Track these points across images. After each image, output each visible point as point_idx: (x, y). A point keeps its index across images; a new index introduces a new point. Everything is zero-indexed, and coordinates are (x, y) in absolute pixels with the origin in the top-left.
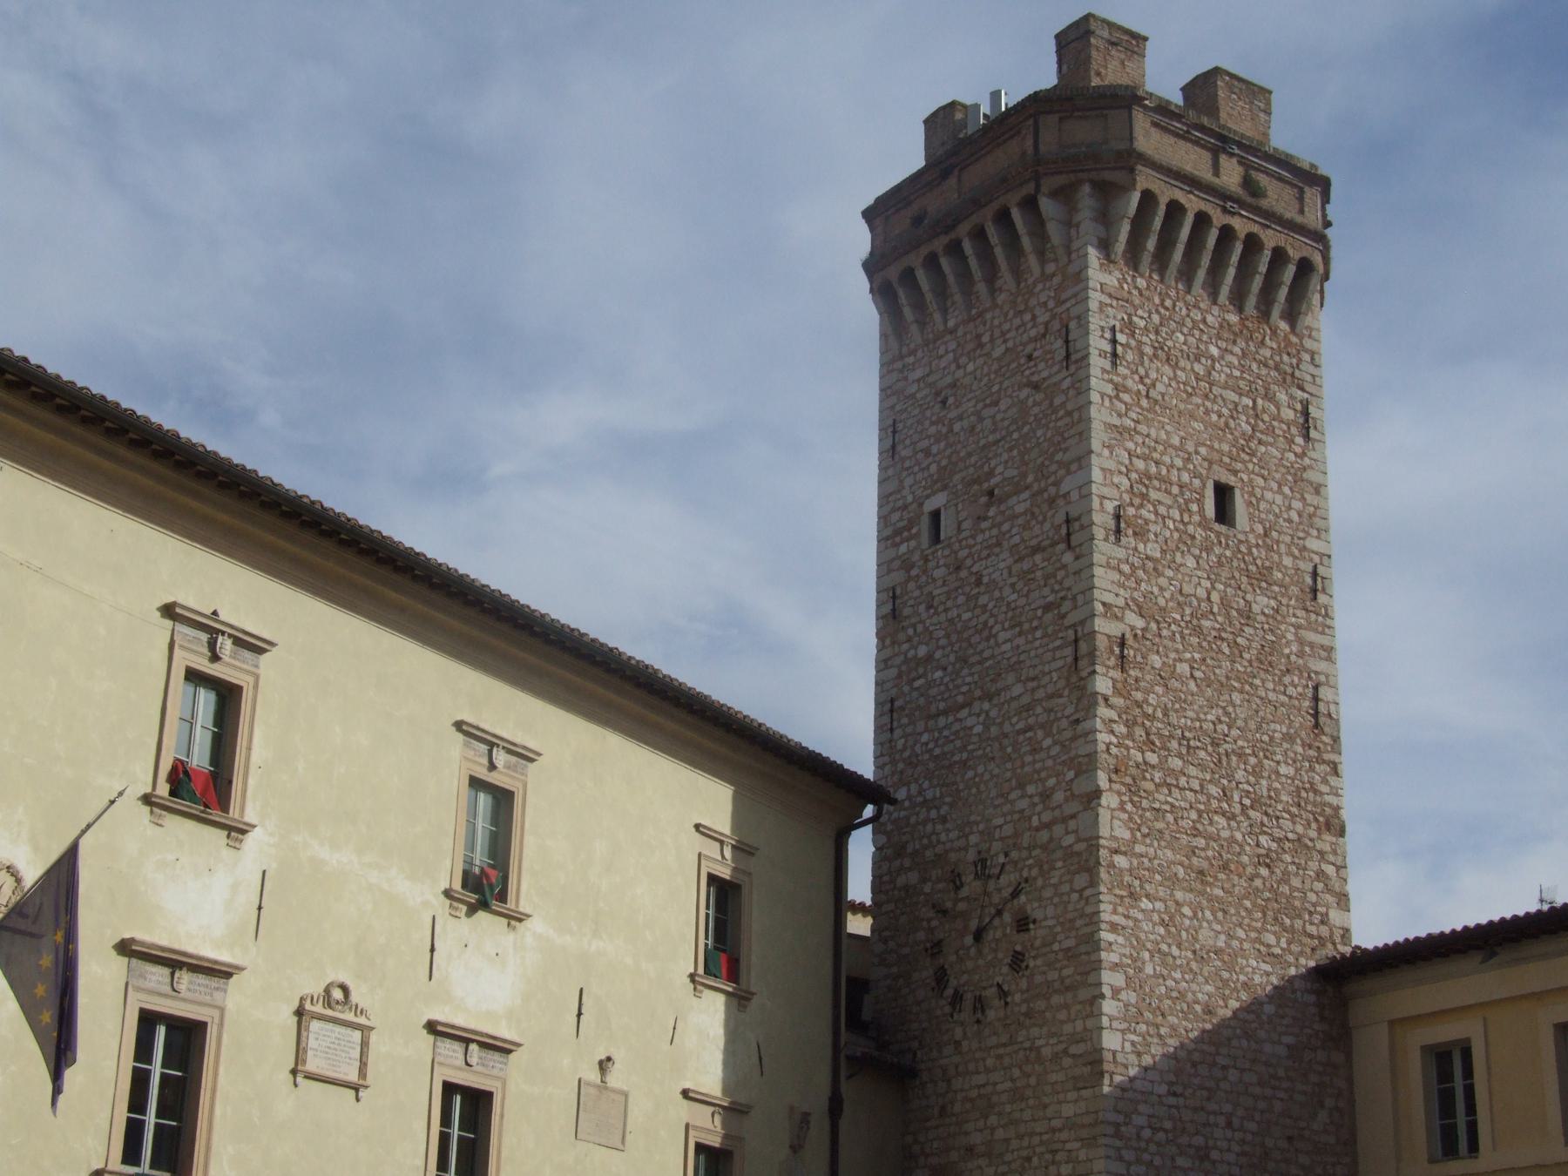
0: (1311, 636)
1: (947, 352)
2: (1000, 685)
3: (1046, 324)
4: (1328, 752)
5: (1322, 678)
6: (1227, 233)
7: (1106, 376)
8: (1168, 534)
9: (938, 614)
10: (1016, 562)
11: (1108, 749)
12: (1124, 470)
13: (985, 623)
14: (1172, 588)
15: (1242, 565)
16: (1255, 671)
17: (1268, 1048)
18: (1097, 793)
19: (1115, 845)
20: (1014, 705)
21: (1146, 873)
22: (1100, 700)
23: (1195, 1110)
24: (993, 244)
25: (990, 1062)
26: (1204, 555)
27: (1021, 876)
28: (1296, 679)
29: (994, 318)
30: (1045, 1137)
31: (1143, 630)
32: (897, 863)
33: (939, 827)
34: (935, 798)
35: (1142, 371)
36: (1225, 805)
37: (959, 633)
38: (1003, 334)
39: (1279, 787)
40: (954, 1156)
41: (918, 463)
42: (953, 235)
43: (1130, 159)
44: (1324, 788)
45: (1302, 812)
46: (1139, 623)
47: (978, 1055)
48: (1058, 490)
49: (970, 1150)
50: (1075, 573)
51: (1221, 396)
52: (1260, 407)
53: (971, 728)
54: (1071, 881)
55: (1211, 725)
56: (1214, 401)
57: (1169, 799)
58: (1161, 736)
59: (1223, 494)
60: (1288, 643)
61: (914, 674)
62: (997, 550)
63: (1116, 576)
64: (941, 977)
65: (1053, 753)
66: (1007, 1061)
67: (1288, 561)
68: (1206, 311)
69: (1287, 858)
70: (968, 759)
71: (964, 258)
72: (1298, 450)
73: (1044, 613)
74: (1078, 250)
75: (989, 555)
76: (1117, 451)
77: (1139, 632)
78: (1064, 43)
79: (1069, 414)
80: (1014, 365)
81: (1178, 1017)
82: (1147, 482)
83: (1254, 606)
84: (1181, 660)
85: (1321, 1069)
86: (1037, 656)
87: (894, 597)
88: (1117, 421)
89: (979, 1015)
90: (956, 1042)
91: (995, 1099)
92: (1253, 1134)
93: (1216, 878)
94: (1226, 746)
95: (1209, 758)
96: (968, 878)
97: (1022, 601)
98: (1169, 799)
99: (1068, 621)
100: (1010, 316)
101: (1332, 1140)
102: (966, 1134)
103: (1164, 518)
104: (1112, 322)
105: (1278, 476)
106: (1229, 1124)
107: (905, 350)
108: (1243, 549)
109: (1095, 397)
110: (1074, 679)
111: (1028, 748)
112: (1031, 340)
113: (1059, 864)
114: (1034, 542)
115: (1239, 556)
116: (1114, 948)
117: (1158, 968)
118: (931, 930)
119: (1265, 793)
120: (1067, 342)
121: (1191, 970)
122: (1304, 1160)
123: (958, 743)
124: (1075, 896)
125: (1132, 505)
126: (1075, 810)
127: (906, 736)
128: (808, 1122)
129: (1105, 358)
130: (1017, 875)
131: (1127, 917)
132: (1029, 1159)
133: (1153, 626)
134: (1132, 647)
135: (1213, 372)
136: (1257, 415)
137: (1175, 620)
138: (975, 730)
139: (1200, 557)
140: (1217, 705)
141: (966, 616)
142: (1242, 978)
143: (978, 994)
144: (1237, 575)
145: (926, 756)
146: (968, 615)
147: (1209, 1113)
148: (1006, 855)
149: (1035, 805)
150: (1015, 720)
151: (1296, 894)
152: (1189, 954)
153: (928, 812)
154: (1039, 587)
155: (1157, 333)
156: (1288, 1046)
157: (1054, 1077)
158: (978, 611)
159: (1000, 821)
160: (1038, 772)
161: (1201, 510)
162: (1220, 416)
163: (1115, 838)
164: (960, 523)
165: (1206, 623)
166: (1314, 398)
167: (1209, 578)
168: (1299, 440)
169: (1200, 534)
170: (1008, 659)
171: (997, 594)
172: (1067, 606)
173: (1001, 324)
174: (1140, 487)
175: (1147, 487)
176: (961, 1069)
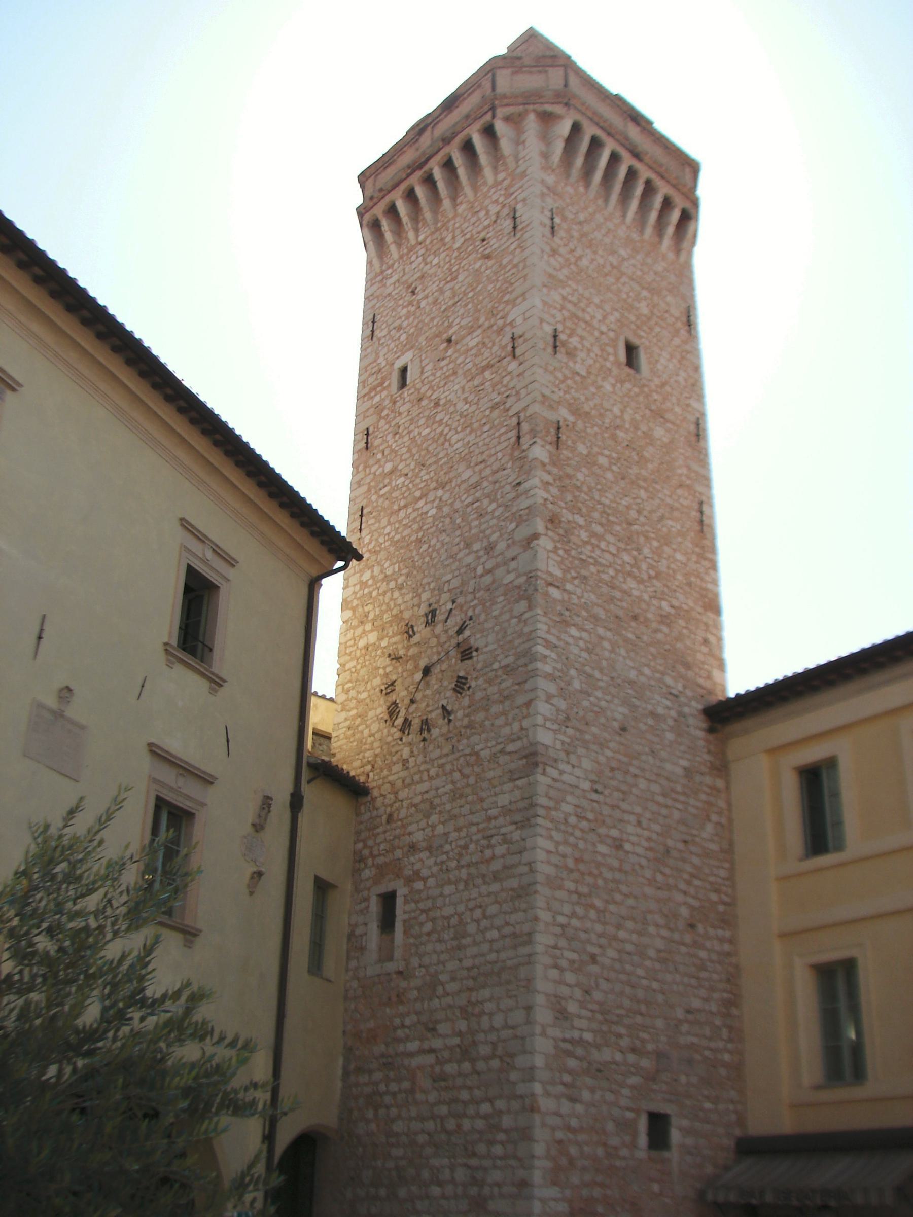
0: (695, 467)
2: (452, 474)
17: (668, 766)
19: (550, 579)
23: (614, 807)
32: (359, 631)
40: (398, 853)
42: (426, 168)
44: (707, 578)
46: (571, 419)
47: (422, 768)
49: (413, 848)
50: (518, 376)
53: (426, 513)
54: (511, 610)
59: (631, 350)
65: (496, 514)
75: (446, 384)
79: (516, 266)
86: (484, 445)
89: (425, 734)
91: (437, 801)
97: (474, 407)
102: (410, 834)
107: (384, 267)
111: (475, 516)
112: (485, 228)
114: (484, 363)
122: (696, 860)
124: (515, 621)
126: (515, 554)
128: (269, 806)
130: (463, 615)
131: (559, 639)
132: (466, 847)
142: (650, 707)
143: (425, 717)
146: (428, 430)
148: (454, 602)
149: (479, 558)
156: (685, 769)
159: (449, 577)
160: (484, 532)
161: (616, 354)
163: (551, 574)
164: (423, 368)
169: (615, 371)
171: (452, 409)
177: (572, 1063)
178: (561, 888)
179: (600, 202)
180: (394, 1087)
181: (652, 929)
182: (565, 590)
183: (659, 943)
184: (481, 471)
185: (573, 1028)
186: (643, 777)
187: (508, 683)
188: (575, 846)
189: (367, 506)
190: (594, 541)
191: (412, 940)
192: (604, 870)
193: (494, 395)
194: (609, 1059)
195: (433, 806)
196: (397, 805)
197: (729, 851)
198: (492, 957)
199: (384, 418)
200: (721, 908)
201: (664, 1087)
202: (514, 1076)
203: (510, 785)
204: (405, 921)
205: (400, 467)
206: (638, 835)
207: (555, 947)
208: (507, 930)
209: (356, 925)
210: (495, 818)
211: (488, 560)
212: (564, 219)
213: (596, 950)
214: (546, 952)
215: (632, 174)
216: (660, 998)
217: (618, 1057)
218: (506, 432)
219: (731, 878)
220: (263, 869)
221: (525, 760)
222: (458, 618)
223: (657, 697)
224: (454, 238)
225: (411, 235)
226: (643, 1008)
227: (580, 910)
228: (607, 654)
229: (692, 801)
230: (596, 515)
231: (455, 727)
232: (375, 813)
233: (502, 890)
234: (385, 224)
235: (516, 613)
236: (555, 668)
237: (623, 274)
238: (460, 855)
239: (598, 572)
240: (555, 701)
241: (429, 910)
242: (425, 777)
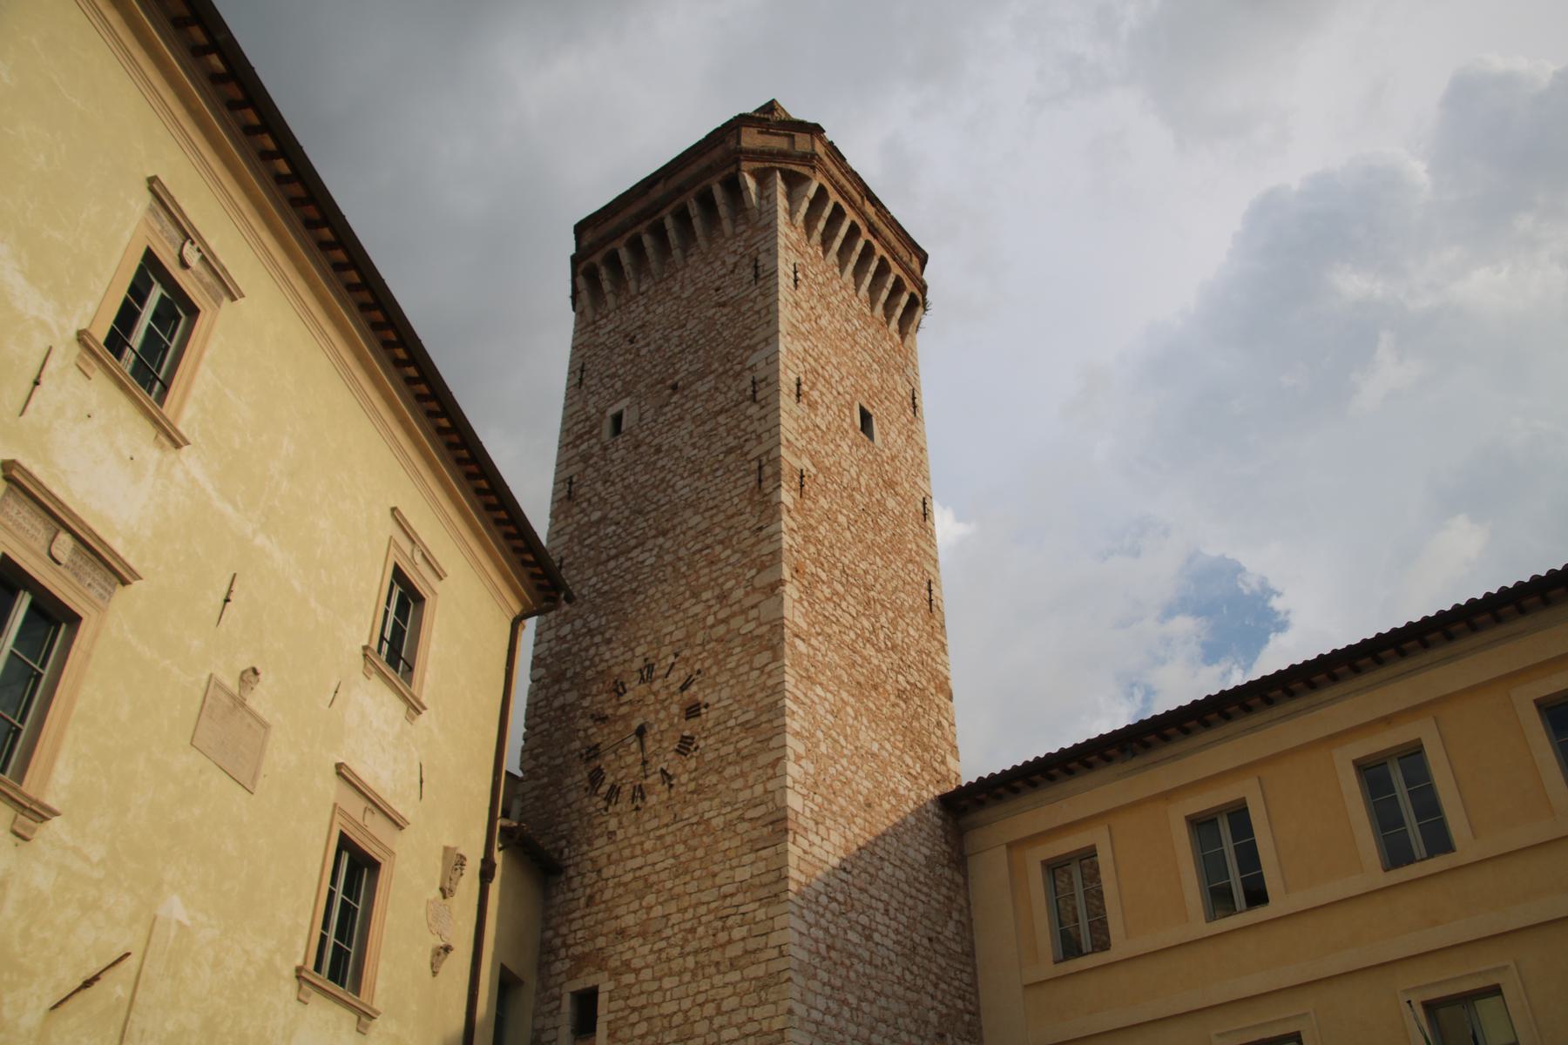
2: (676, 521)
18: (781, 582)
23: (862, 890)
24: (692, 215)
25: (648, 845)
27: (692, 669)
33: (603, 649)
34: (600, 626)
40: (601, 942)
44: (939, 660)
46: (813, 470)
47: (634, 841)
49: (622, 933)
50: (759, 419)
54: (751, 662)
59: (866, 417)
61: (585, 536)
64: (596, 777)
66: (669, 840)
70: (638, 587)
75: (670, 430)
79: (758, 312)
87: (571, 483)
89: (639, 802)
90: (610, 833)
102: (617, 917)
106: (887, 912)
112: (720, 277)
123: (629, 577)
124: (756, 673)
130: (688, 670)
131: (805, 695)
132: (693, 930)
138: (647, 563)
142: (892, 785)
143: (638, 783)
147: (871, 897)
148: (676, 655)
158: (656, 472)
159: (672, 628)
163: (796, 625)
164: (642, 414)
169: (851, 433)
171: (677, 454)
178: (814, 977)
179: (837, 270)
182: (810, 645)
184: (712, 517)
186: (888, 860)
188: (827, 930)
190: (835, 598)
193: (730, 439)
195: (649, 886)
196: (600, 884)
197: (970, 954)
199: (591, 466)
200: (967, 1017)
203: (752, 857)
204: (609, 1022)
205: (610, 516)
206: (888, 927)
208: (750, 1028)
209: (543, 1030)
210: (732, 895)
211: (721, 608)
212: (806, 276)
215: (868, 250)
218: (743, 477)
219: (974, 984)
221: (770, 827)
222: (682, 672)
223: (898, 775)
224: (682, 287)
225: (632, 285)
228: (851, 721)
230: (837, 573)
231: (678, 793)
232: (570, 895)
233: (743, 979)
234: (604, 273)
235: (757, 664)
236: (802, 727)
237: (856, 343)
238: (686, 940)
240: (803, 762)
241: (643, 1007)
242: (638, 851)
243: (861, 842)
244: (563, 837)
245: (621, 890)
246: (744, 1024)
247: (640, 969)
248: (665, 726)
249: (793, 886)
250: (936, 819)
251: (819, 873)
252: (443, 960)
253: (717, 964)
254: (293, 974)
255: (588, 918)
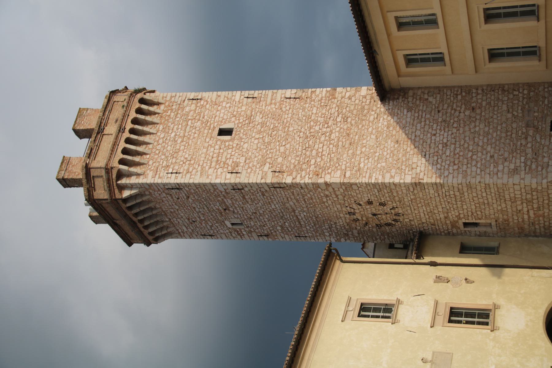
1: (177, 221)
2: (290, 207)
3: (166, 194)
4: (308, 94)
5: (283, 96)
6: (132, 131)
7: (184, 177)
8: (237, 154)
9: (266, 224)
10: (248, 203)
11: (310, 178)
12: (216, 170)
13: (269, 211)
14: (255, 153)
15: (246, 126)
16: (282, 122)
18: (326, 184)
19: (343, 176)
20: (296, 204)
21: (352, 164)
22: (294, 181)
23: (430, 147)
24: (139, 210)
26: (243, 140)
28: (284, 106)
29: (165, 208)
30: (441, 198)
31: (270, 165)
34: (329, 226)
35: (181, 163)
36: (327, 134)
37: (273, 218)
38: (170, 206)
39: (320, 113)
40: (448, 222)
41: (215, 229)
42: (137, 222)
43: (108, 170)
44: (320, 96)
45: (329, 105)
46: (267, 165)
47: (414, 215)
48: (224, 192)
50: (252, 187)
51: (188, 132)
52: (192, 118)
54: (355, 190)
55: (301, 139)
56: (190, 135)
57: (326, 156)
58: (304, 159)
60: (272, 108)
61: (287, 231)
62: (244, 208)
63: (252, 174)
66: (416, 208)
67: (244, 108)
68: (159, 137)
69: (344, 111)
71: (145, 218)
72: (205, 103)
73: (265, 196)
74: (141, 185)
75: (246, 210)
76: (209, 173)
77: (271, 166)
78: (67, 185)
80: (181, 203)
81: (399, 154)
82: (219, 162)
83: (259, 122)
84: (279, 150)
85: (415, 99)
86: (280, 198)
87: (261, 236)
88: (199, 173)
89: (401, 215)
92: (437, 126)
93: (352, 138)
94: (307, 133)
95: (312, 140)
96: (355, 217)
97: (261, 201)
98: (326, 156)
99: (268, 190)
100: (164, 204)
101: (439, 96)
102: (440, 219)
103: (231, 156)
104: (165, 174)
105: (215, 112)
106: (435, 135)
108: (240, 125)
109: (191, 181)
110: (287, 188)
113: (350, 193)
114: (242, 198)
115: (243, 127)
116: (377, 178)
117: (383, 161)
118: (373, 227)
119: (323, 119)
120: (173, 189)
121: (384, 148)
122: (446, 106)
123: (310, 219)
125: (227, 168)
127: (308, 233)
129: (178, 177)
131: (366, 172)
132: (449, 202)
133: (268, 160)
134: (276, 168)
135: (180, 135)
136: (194, 118)
137: (266, 152)
139: (244, 142)
140: (294, 136)
141: (267, 216)
142: (385, 129)
144: (249, 128)
145: (314, 227)
147: (431, 142)
148: (347, 207)
149: (330, 199)
150: (301, 204)
151: (356, 108)
152: (378, 149)
153: (333, 227)
154: (257, 197)
155: (168, 156)
157: (421, 196)
158: (265, 213)
159: (336, 209)
160: (319, 198)
162: (195, 133)
163: (340, 176)
164: (235, 218)
165: (266, 140)
166: (187, 97)
167: (251, 138)
168: (202, 102)
169: (236, 142)
170: (281, 205)
171: (259, 208)
172: (262, 190)
173: (167, 206)
174: (221, 164)
175: (221, 162)
176: (419, 219)
177: (534, 166)
178: (466, 171)
180: (542, 222)
181: (477, 129)
183: (482, 126)
185: (520, 166)
187: (386, 191)
189: (295, 235)
190: (320, 155)
191: (484, 218)
192: (456, 152)
194: (530, 150)
198: (493, 195)
200: (464, 94)
201: (540, 123)
202: (540, 188)
204: (476, 220)
207: (490, 174)
208: (483, 190)
210: (439, 194)
213: (489, 155)
214: (492, 178)
216: (504, 125)
217: (529, 145)
220: (465, 278)
223: (380, 124)
226: (509, 134)
227: (474, 163)
229: (421, 108)
232: (430, 229)
233: (467, 192)
239: (333, 153)
241: (472, 212)
242: (419, 214)
243: (413, 147)
244: (409, 232)
245: (431, 218)
246: (482, 192)
247: (459, 213)
248: (374, 209)
249: (438, 181)
250: (391, 104)
251: (430, 168)
252: (469, 280)
253: (461, 197)
254: (493, 332)
255: (439, 225)
